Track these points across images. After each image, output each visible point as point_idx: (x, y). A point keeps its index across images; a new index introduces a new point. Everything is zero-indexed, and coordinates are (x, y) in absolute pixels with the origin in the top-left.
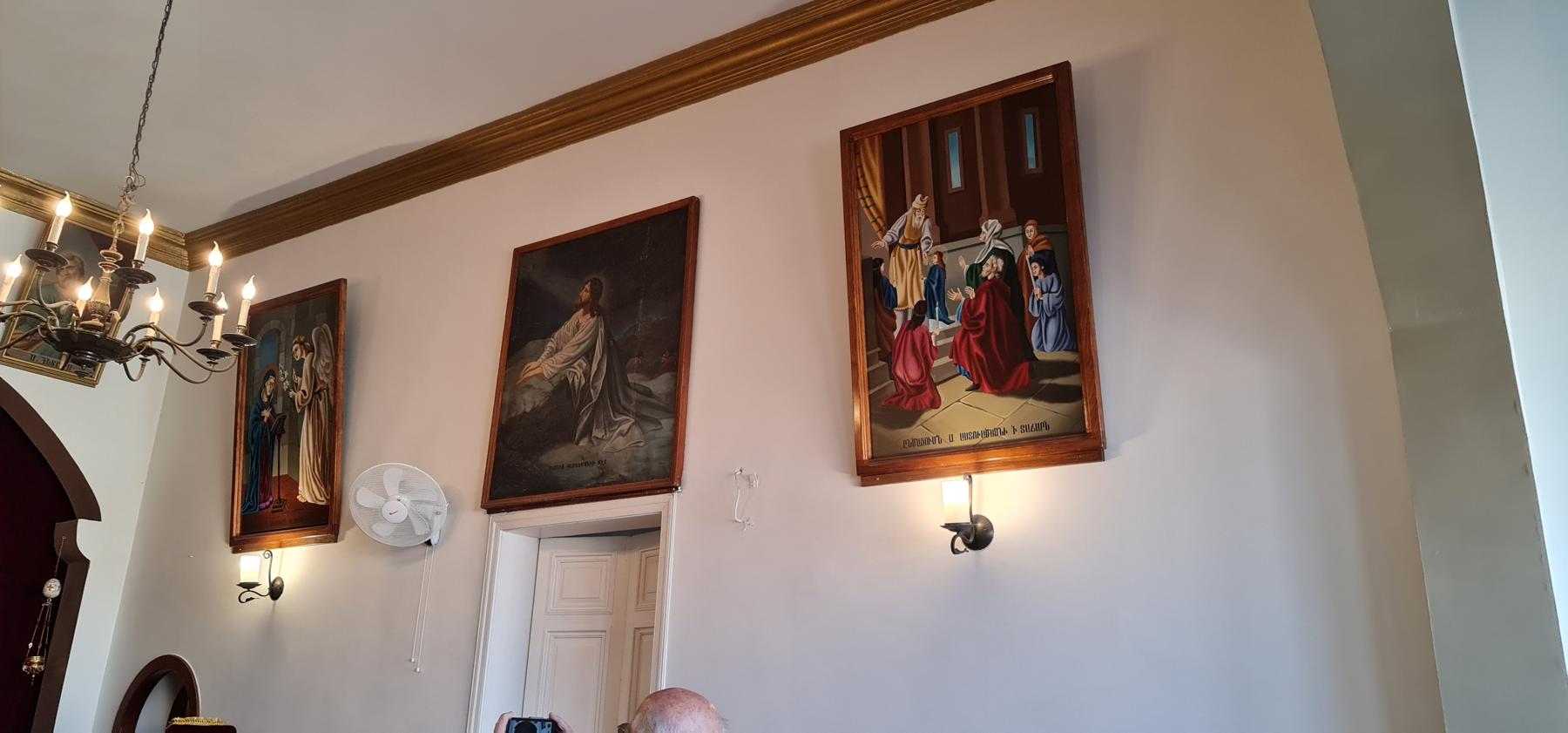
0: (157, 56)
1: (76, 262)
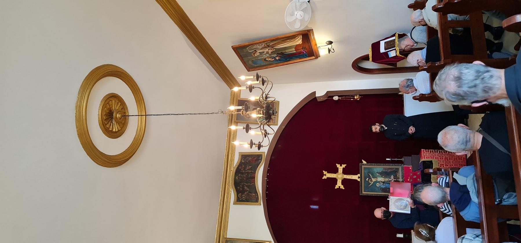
0: (184, 114)
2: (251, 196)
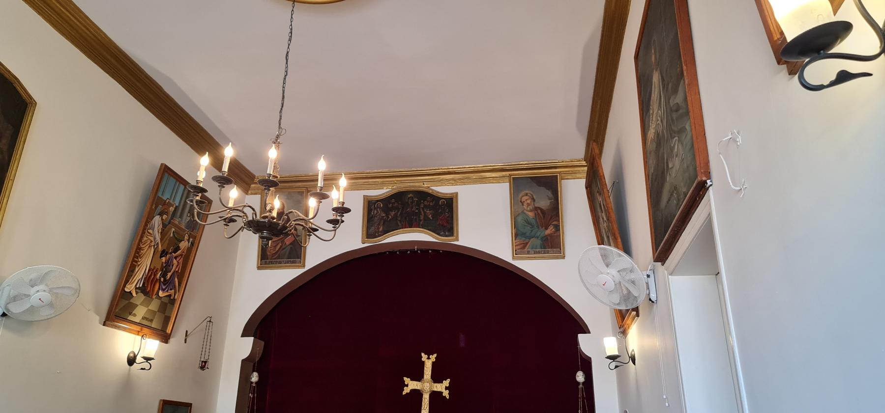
1: (529, 196)
2: (379, 224)
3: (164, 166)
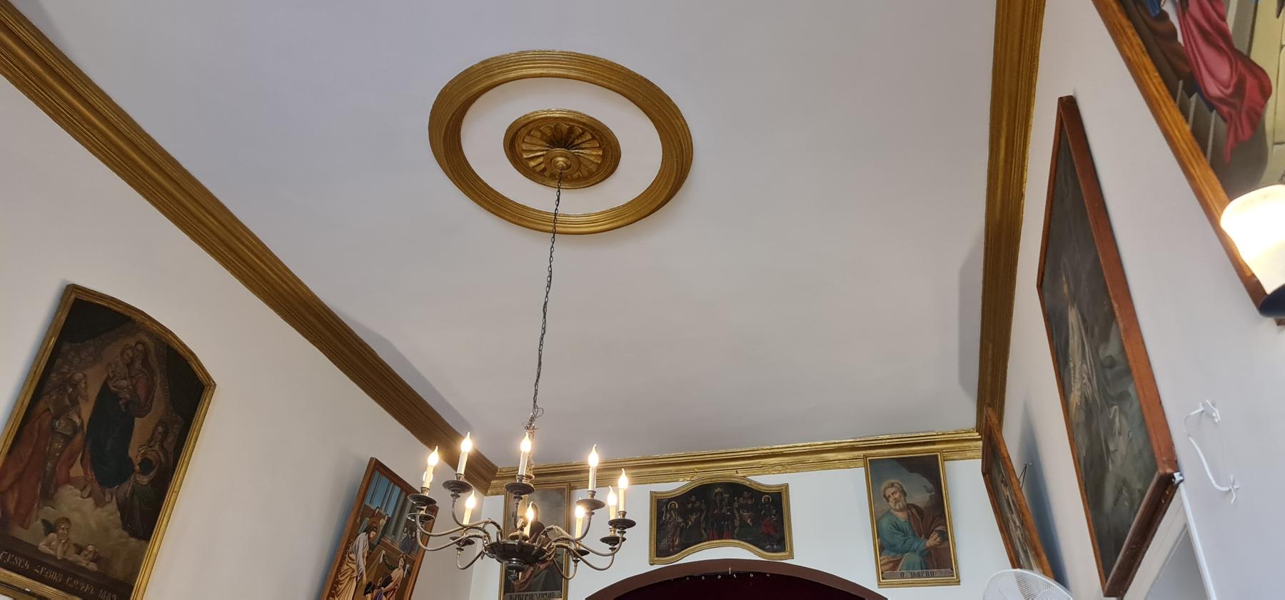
1: (896, 487)
2: (673, 535)
3: (374, 461)
